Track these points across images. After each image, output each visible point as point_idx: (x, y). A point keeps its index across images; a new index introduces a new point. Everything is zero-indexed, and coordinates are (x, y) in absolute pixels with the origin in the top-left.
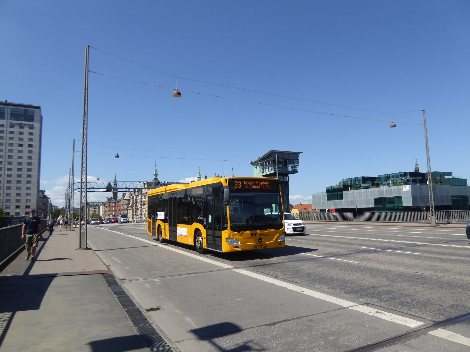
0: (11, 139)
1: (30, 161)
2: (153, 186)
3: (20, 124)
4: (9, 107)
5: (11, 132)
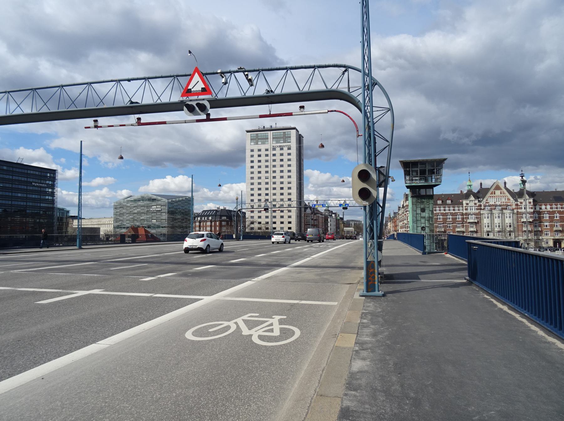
0: (274, 160)
3: (280, 146)
4: (272, 132)
5: (274, 155)
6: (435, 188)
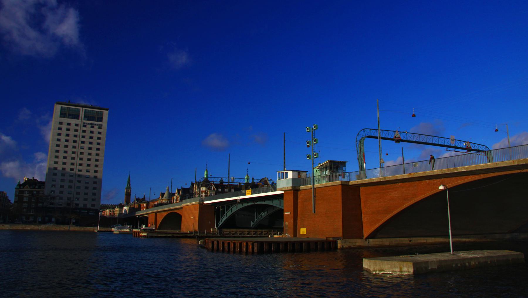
4: (84, 109)
5: (84, 131)
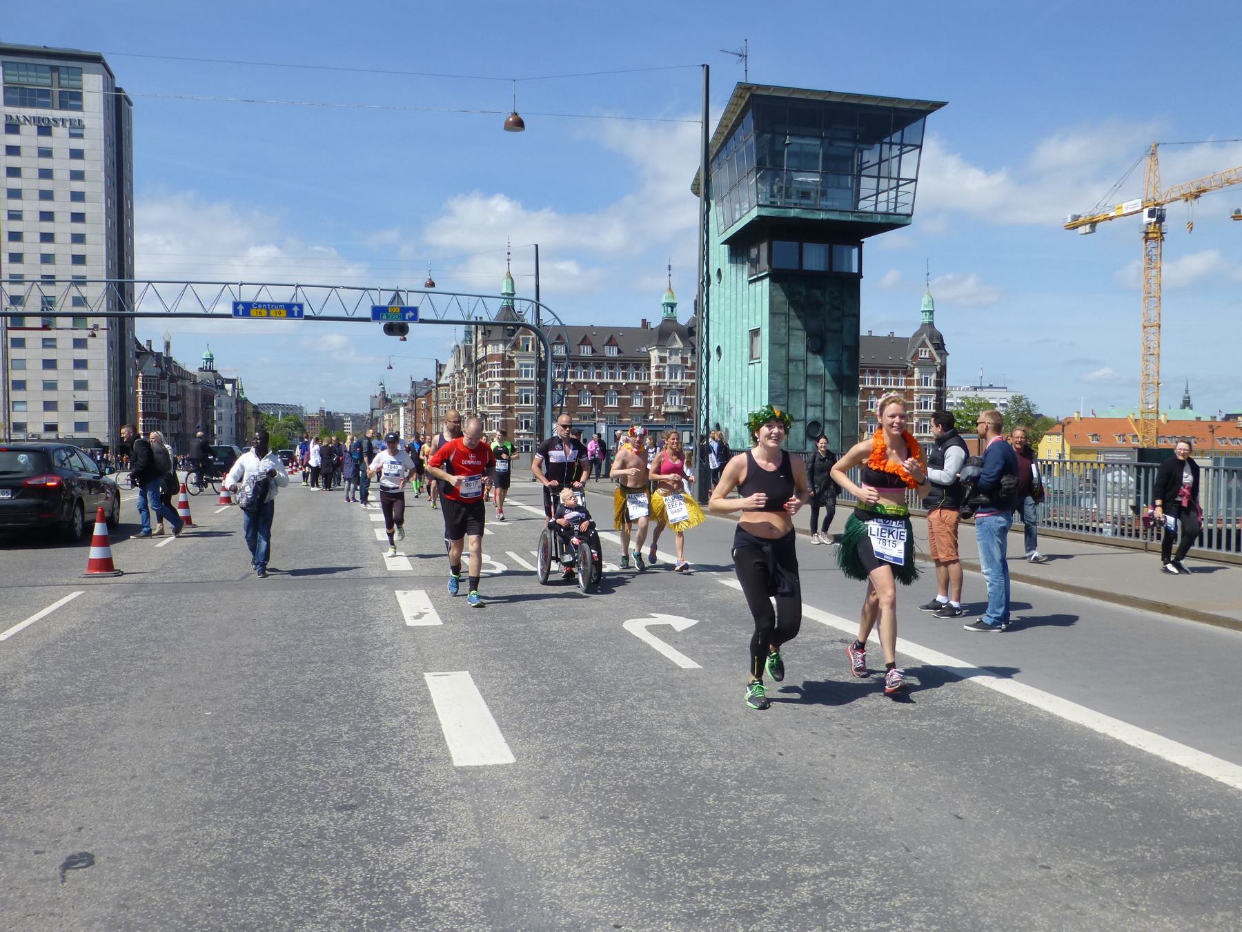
1: (78, 249)
2: (497, 333)
3: (37, 120)
6: (868, 242)
